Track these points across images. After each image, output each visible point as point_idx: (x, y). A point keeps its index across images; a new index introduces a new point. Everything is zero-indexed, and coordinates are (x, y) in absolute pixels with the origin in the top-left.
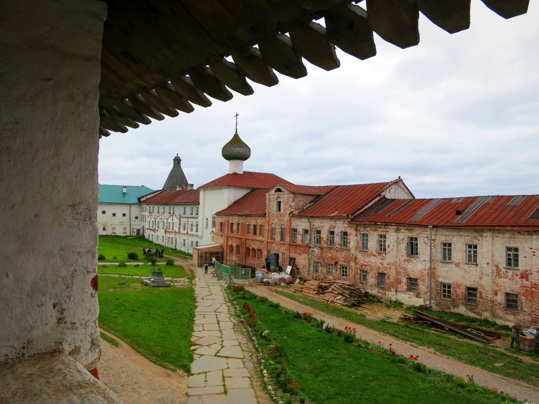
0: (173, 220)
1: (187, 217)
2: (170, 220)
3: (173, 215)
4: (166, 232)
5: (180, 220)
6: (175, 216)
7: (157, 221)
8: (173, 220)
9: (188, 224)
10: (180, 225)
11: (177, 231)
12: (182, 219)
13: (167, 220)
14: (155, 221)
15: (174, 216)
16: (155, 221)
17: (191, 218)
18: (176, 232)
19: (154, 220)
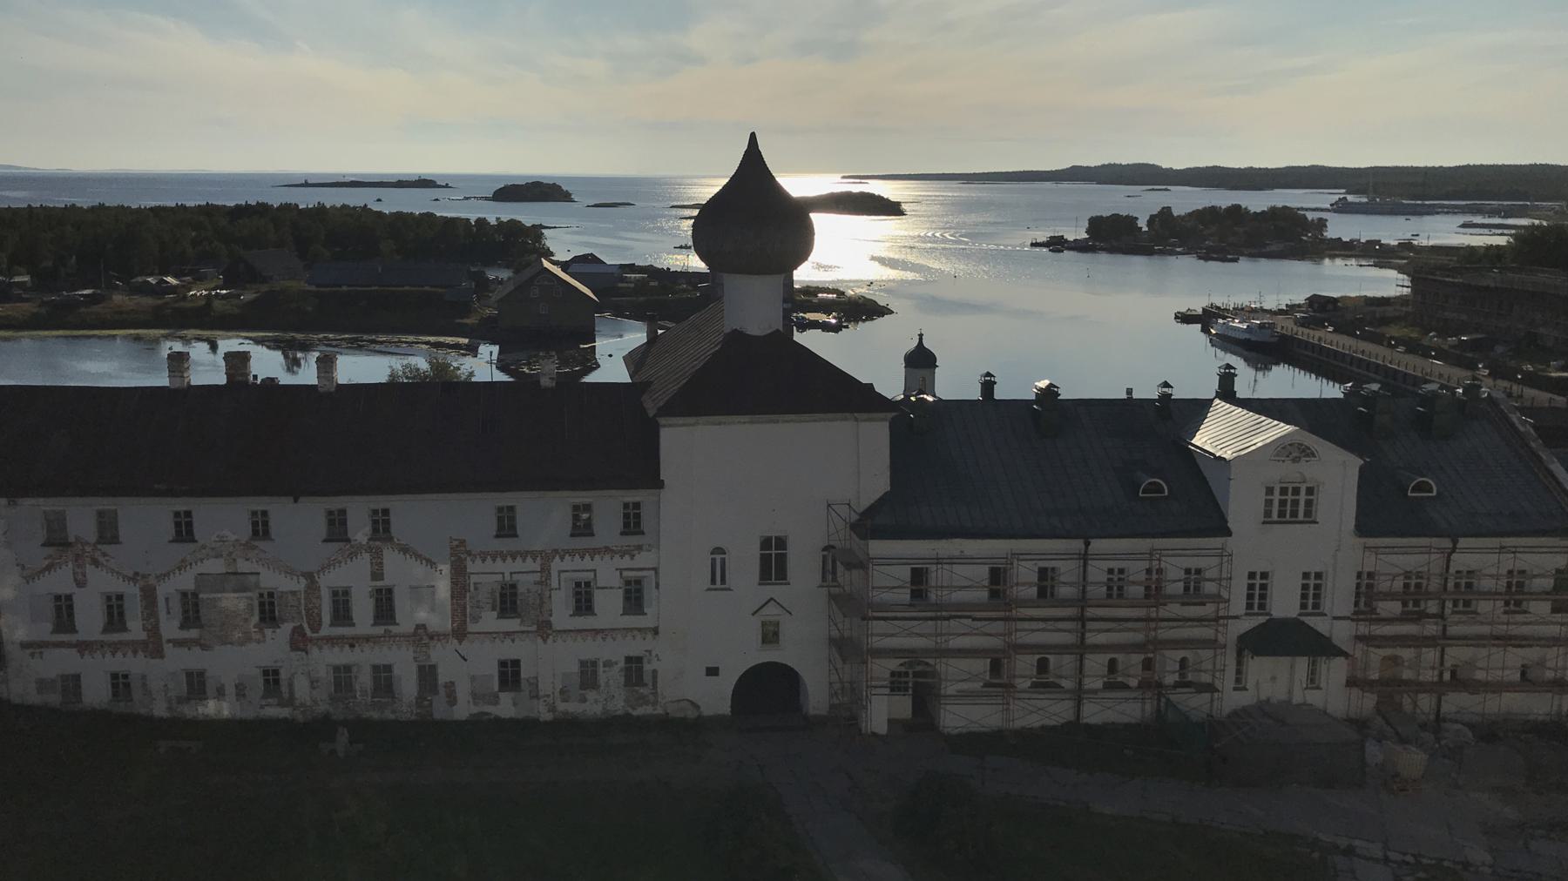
0: (377, 575)
1: (534, 555)
2: (354, 575)
3: (377, 556)
4: (299, 642)
5: (459, 572)
6: (405, 550)
7: (164, 590)
8: (377, 575)
9: (544, 582)
10: (460, 588)
11: (439, 621)
12: (473, 566)
13: (310, 576)
14: (149, 596)
15: (391, 558)
16: (149, 596)
17: (572, 553)
18: (422, 636)
19: (132, 591)
